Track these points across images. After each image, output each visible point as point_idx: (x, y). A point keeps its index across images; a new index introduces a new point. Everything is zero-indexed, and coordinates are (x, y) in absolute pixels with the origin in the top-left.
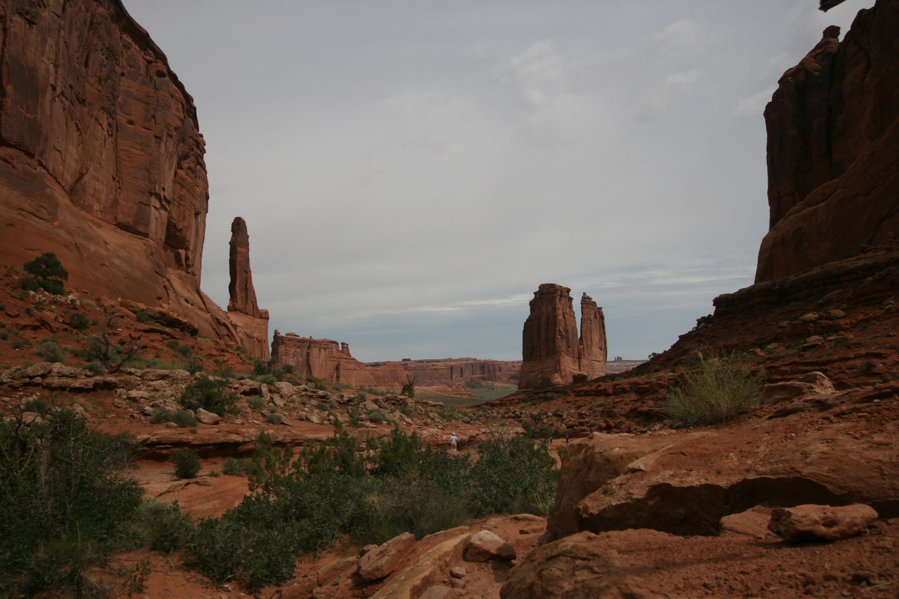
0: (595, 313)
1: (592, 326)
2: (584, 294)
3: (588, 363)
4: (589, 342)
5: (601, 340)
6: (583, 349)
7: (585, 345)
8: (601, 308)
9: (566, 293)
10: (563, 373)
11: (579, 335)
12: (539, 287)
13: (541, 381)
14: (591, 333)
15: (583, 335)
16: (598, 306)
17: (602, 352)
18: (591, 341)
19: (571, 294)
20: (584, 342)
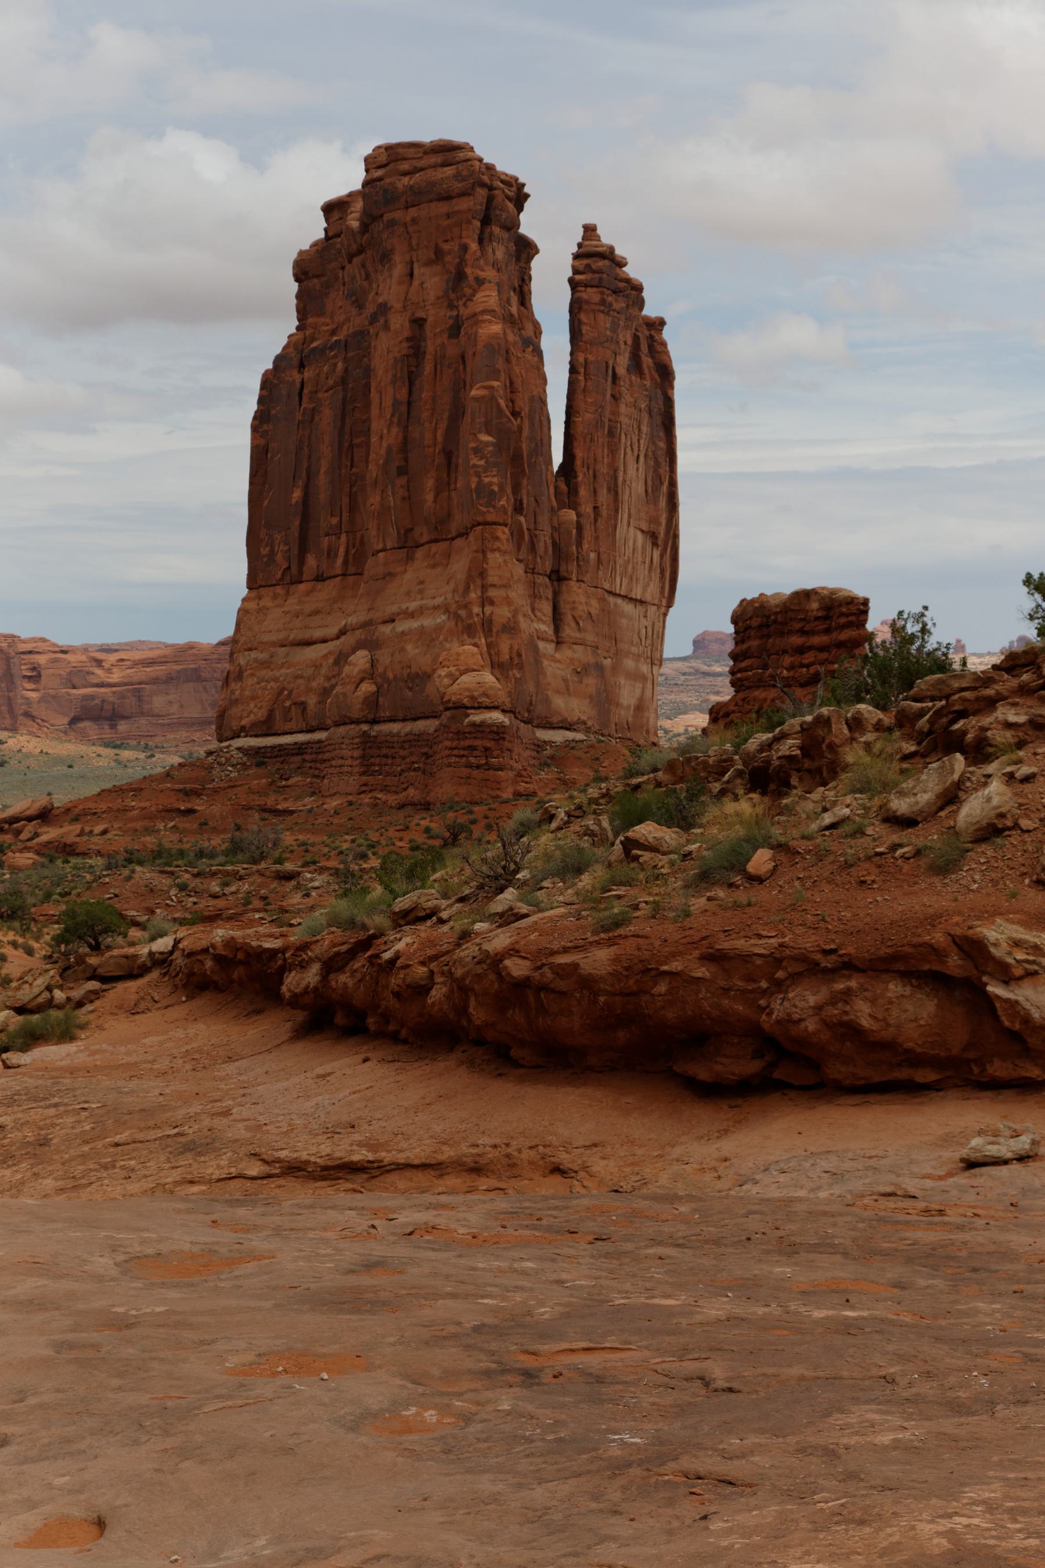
0: (636, 339)
1: (623, 409)
2: (590, 231)
3: (595, 607)
4: (604, 497)
5: (656, 489)
6: (579, 527)
7: (587, 509)
8: (661, 323)
9: (511, 206)
10: (505, 645)
11: (557, 457)
12: (370, 163)
13: (367, 688)
14: (613, 451)
15: (579, 453)
16: (650, 311)
17: (656, 554)
18: (614, 491)
19: (529, 224)
20: (583, 492)
